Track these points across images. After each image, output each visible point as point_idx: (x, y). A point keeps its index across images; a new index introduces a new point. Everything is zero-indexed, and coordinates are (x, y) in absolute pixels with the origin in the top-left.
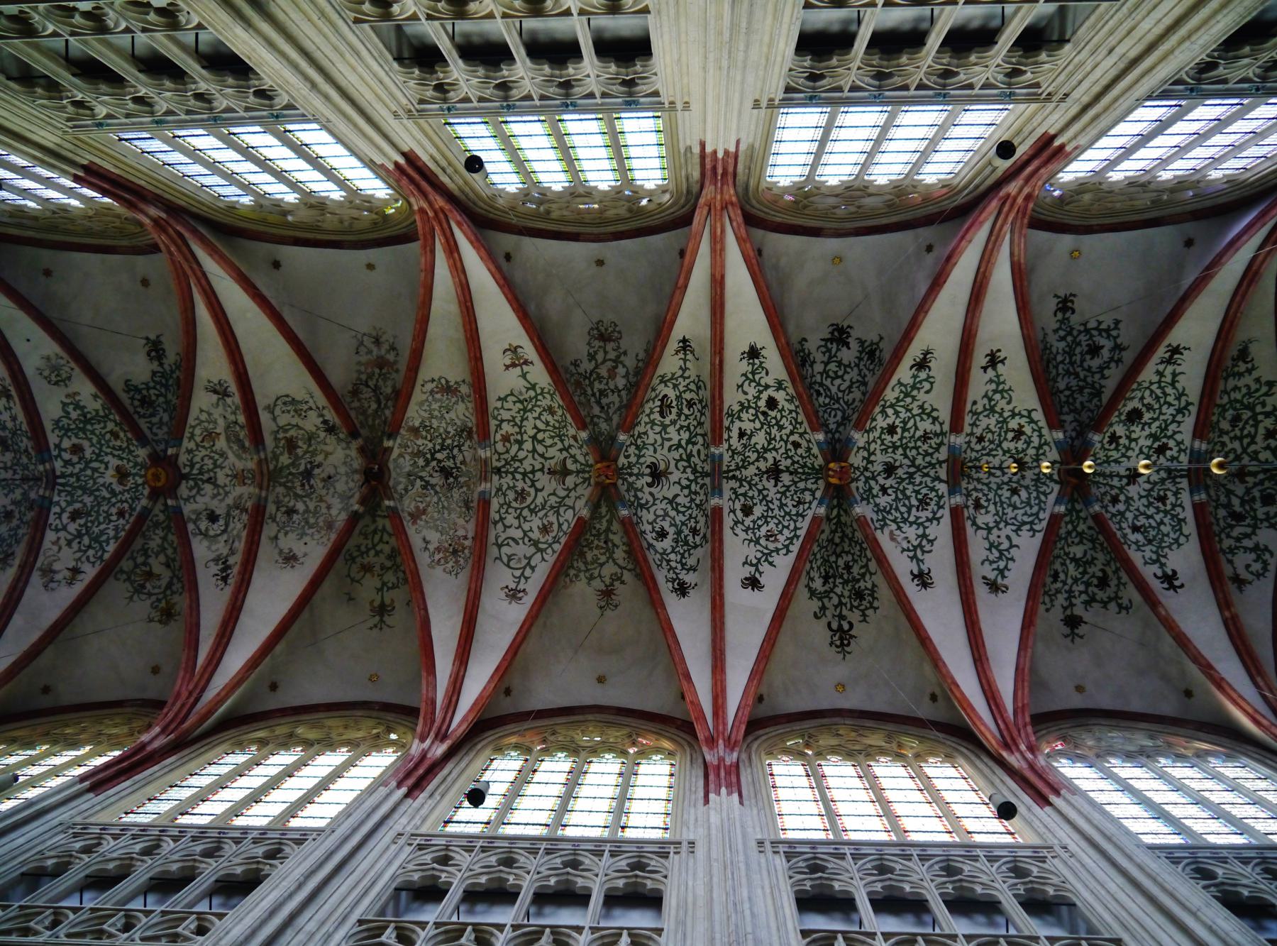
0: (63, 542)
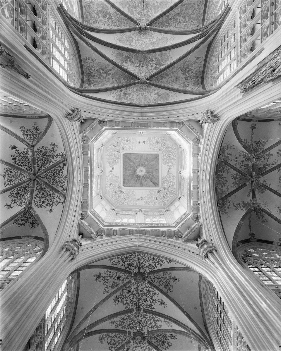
0: (121, 317)
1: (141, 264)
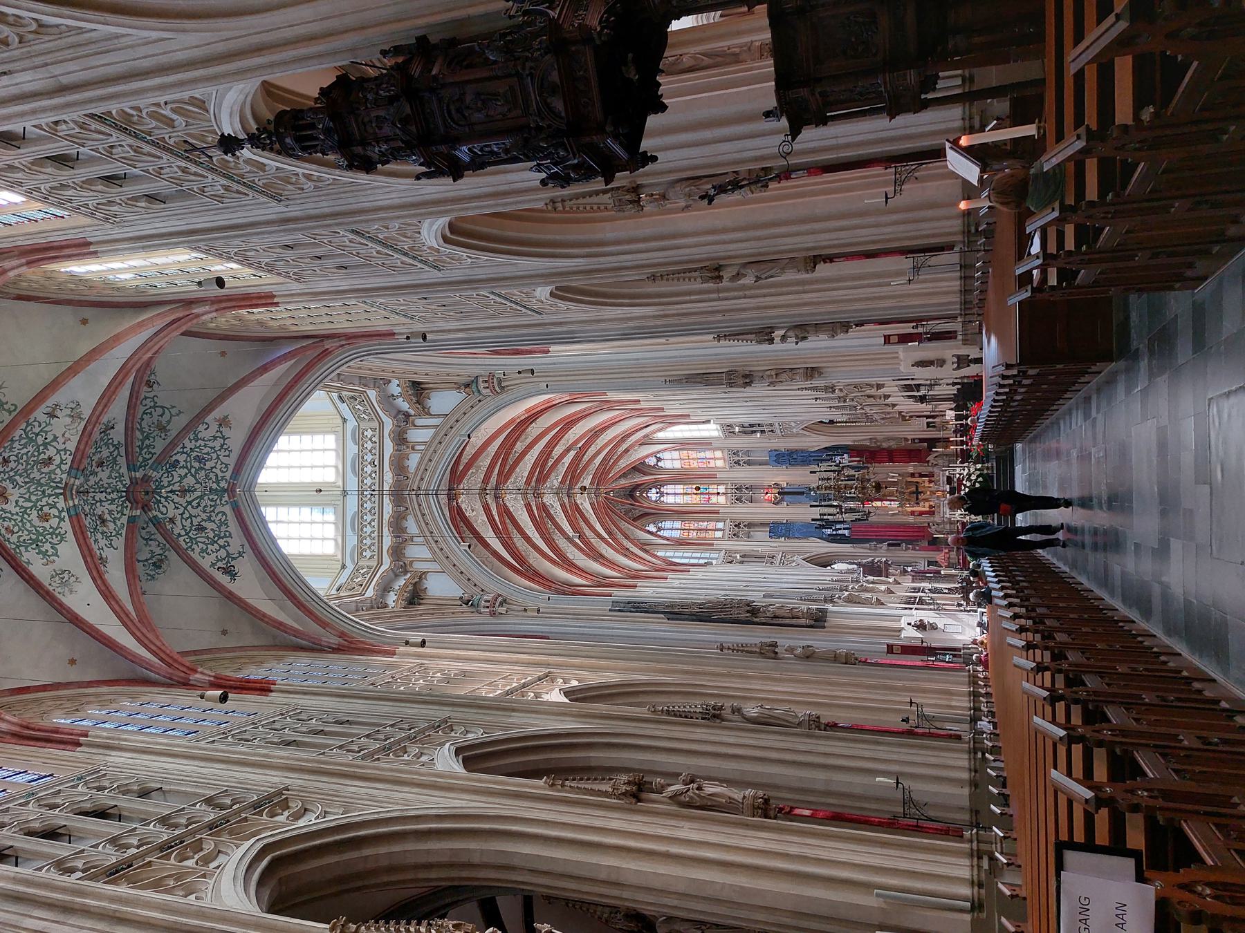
0: (61, 440)
1: (166, 498)
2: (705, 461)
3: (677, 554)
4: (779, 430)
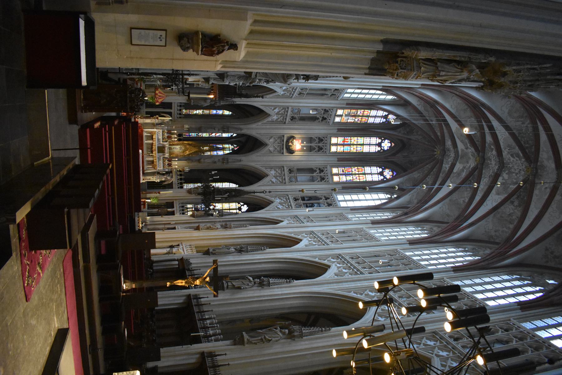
2: (346, 172)
3: (375, 97)
4: (291, 200)
